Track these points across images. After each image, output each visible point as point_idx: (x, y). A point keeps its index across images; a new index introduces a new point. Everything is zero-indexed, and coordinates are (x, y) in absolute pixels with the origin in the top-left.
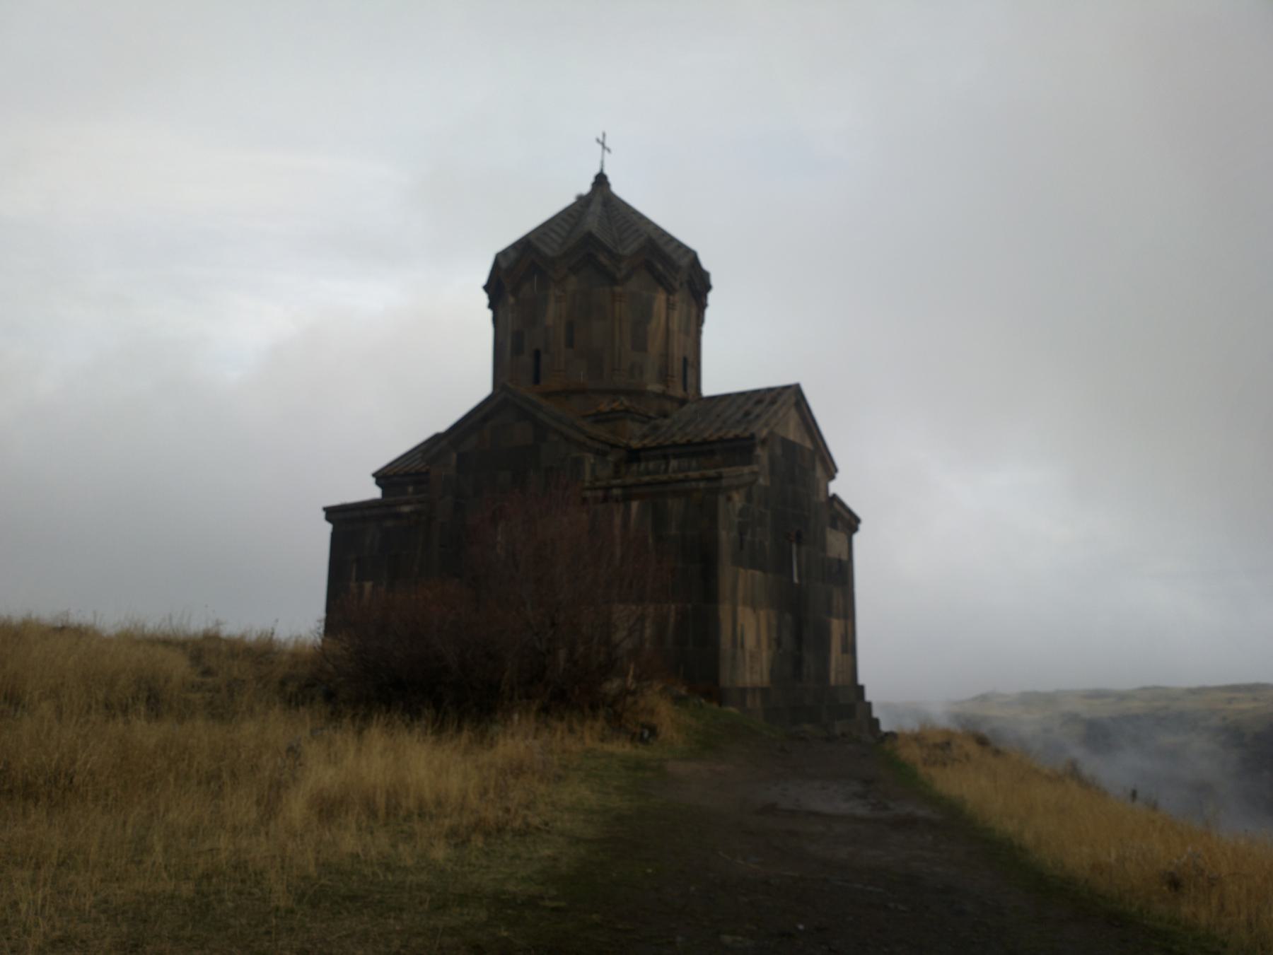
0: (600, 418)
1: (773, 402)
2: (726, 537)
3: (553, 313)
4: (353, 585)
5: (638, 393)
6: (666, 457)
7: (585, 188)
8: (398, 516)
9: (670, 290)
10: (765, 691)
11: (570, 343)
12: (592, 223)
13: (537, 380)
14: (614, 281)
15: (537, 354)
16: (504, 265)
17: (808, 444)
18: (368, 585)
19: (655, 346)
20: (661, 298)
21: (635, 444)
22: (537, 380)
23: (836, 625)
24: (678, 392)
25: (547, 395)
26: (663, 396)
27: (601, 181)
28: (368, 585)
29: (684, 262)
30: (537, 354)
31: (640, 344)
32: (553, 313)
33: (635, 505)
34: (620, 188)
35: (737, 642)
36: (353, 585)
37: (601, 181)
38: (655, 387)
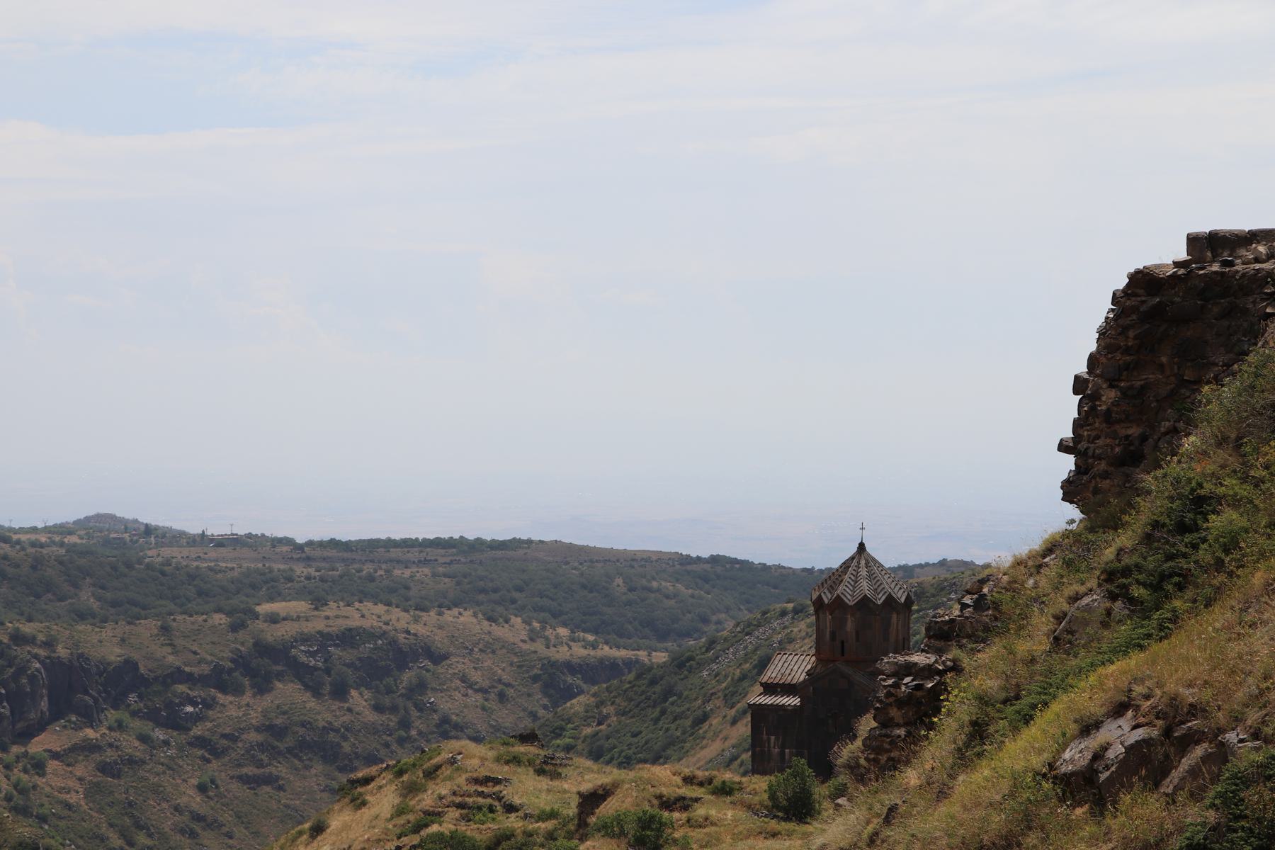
3: (850, 625)
4: (765, 737)
7: (853, 549)
11: (857, 640)
12: (865, 587)
13: (843, 654)
15: (843, 642)
16: (826, 601)
18: (773, 738)
22: (843, 654)
27: (862, 547)
28: (773, 738)
29: (903, 600)
30: (843, 642)
32: (850, 625)
36: (765, 737)
37: (862, 547)
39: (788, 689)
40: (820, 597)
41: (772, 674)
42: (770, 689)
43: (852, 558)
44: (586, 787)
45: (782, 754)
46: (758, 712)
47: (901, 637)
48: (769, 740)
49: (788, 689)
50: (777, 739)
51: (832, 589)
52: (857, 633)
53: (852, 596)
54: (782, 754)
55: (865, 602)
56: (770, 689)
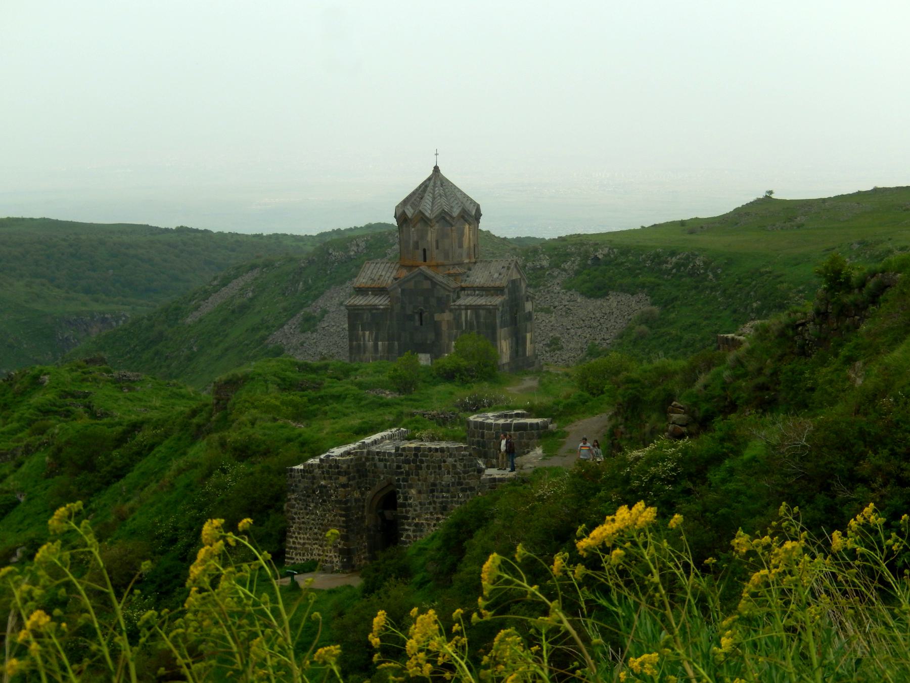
0: (449, 275)
1: (508, 268)
2: (498, 321)
3: (431, 235)
4: (360, 333)
5: (460, 264)
6: (475, 291)
7: (431, 172)
8: (377, 309)
9: (470, 224)
10: (508, 364)
11: (437, 248)
13: (425, 261)
14: (452, 226)
15: (424, 251)
17: (519, 277)
18: (367, 333)
19: (466, 245)
20: (467, 227)
21: (463, 284)
22: (425, 261)
23: (528, 336)
24: (473, 260)
25: (429, 266)
26: (470, 263)
27: (436, 169)
29: (473, 213)
30: (424, 251)
31: (461, 246)
33: (469, 311)
34: (443, 171)
35: (502, 351)
36: (360, 333)
37: (436, 169)
38: (466, 261)
39: (380, 291)
40: (404, 213)
41: (362, 280)
42: (361, 291)
43: (429, 179)
44: (222, 377)
45: (376, 346)
46: (354, 314)
47: (472, 245)
48: (364, 335)
49: (380, 291)
50: (371, 333)
51: (414, 206)
52: (437, 242)
53: (432, 211)
54: (376, 346)
55: (444, 217)
56: (361, 291)
